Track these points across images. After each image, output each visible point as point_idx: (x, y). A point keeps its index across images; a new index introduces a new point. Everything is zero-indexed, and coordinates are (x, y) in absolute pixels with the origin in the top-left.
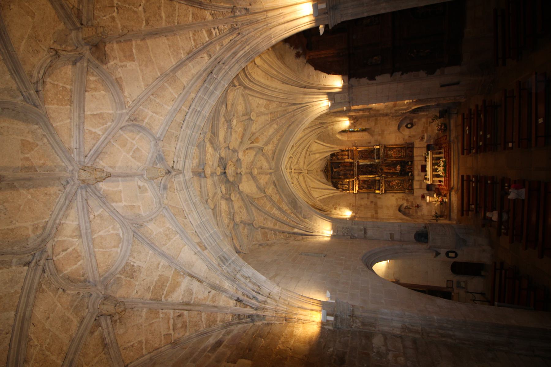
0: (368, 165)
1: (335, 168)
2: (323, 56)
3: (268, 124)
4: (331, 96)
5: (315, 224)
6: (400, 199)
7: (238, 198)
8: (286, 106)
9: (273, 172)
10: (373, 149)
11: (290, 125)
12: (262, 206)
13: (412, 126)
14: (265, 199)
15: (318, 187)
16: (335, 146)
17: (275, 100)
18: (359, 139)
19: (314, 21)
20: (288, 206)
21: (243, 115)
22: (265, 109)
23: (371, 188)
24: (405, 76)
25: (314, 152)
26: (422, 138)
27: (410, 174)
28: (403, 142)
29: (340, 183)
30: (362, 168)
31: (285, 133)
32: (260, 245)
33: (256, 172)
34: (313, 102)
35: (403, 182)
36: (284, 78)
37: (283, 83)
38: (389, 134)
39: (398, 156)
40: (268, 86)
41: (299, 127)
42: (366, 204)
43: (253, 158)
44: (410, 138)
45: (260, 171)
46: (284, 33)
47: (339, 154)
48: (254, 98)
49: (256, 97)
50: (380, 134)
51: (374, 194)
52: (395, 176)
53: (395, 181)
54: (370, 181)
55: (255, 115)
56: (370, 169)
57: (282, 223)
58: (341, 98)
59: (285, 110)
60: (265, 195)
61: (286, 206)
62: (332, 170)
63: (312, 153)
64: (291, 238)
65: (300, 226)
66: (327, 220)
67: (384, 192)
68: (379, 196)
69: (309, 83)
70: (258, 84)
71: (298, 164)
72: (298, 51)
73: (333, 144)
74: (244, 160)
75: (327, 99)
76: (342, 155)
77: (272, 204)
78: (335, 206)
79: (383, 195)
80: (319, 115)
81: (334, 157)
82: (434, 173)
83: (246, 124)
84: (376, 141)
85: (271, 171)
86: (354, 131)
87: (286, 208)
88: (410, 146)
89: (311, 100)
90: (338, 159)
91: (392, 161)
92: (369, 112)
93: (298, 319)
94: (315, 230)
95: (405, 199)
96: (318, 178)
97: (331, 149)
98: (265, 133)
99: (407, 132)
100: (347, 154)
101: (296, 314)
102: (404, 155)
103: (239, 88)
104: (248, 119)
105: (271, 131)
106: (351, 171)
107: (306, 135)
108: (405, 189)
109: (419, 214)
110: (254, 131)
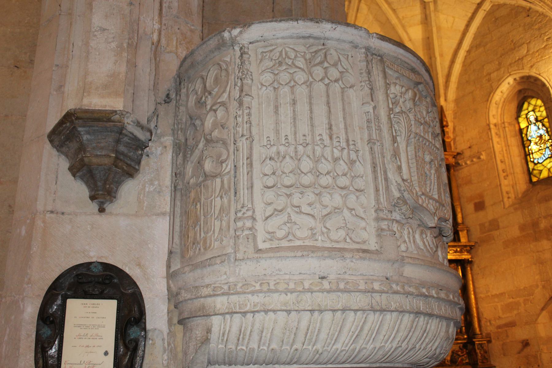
16: (452, 94)
18: (499, 162)
44: (520, 346)
50: (535, 224)
84: (494, 225)
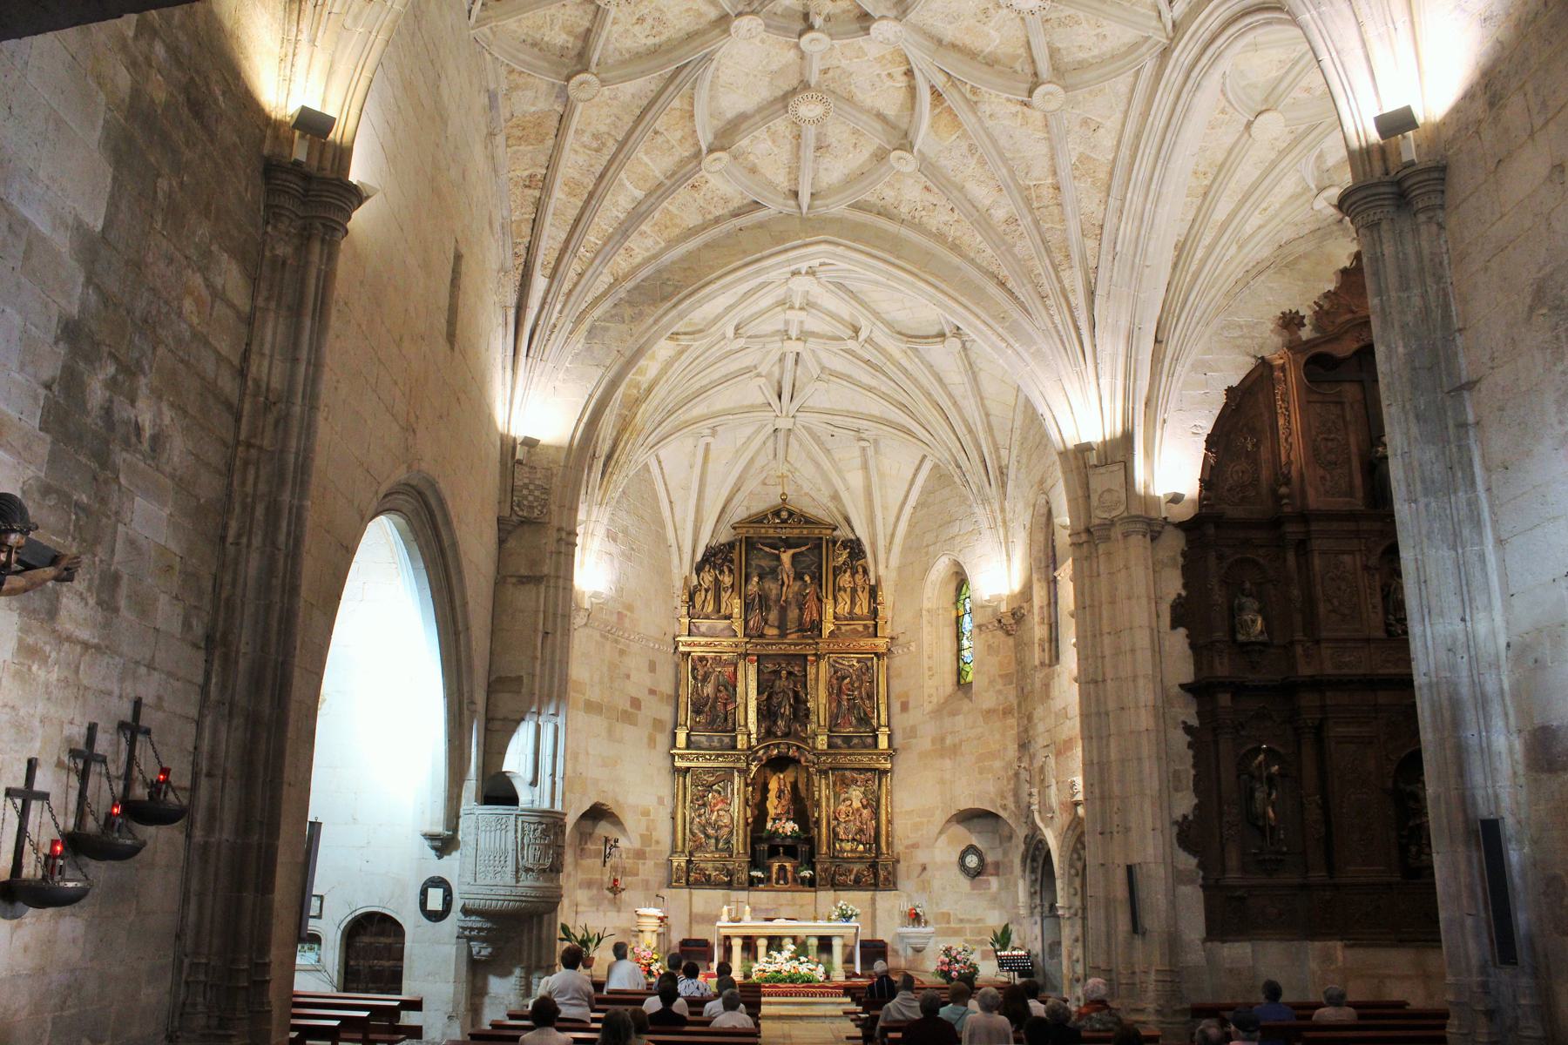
0: (806, 701)
1: (794, 556)
2: (1281, 422)
3: (1012, 172)
4: (1119, 452)
5: (560, 376)
6: (647, 829)
7: (701, 15)
8: (1084, 259)
9: (799, 207)
10: (875, 722)
11: (1002, 284)
12: (656, 133)
13: (975, 874)
14: (687, 154)
15: (710, 478)
16: (895, 560)
19: (1364, 144)
20: (647, 261)
21: (1053, 53)
23: (697, 711)
24: (1180, 740)
25: (872, 463)
26: (915, 918)
27: (759, 874)
28: (899, 847)
29: (727, 580)
30: (790, 673)
31: (972, 261)
32: (492, 97)
33: (808, 109)
34: (1098, 378)
35: (721, 845)
36: (1200, 254)
37: (1180, 248)
38: (942, 782)
39: (841, 830)
40: (1168, 160)
41: (996, 326)
42: (628, 677)
43: (868, 103)
45: (810, 133)
46: (1332, 50)
47: (859, 577)
48: (1122, 107)
49: (1126, 114)
50: (943, 739)
51: (669, 726)
52: (749, 814)
53: (733, 810)
54: (730, 708)
55: (1053, 106)
56: (786, 710)
57: (577, 221)
58: (1109, 490)
59: (1068, 256)
60: (704, 149)
61: (647, 254)
62: (788, 544)
63: (870, 452)
64: (509, 254)
65: (558, 307)
66: (582, 425)
67: (679, 763)
68: (663, 740)
69: (1175, 359)
70: (1179, 108)
71: (823, 376)
72: (1306, 321)
73: (906, 549)
74: (861, 53)
75: (1107, 438)
76: (854, 590)
78: (620, 535)
79: (668, 763)
80: (1042, 409)
81: (844, 555)
82: (762, 944)
83: (1018, 67)
84: (912, 732)
85: (805, 199)
86: (959, 636)
87: (637, 250)
88: (882, 873)
89: (1105, 368)
90: (837, 571)
91: (818, 804)
92: (1042, 664)
93: (297, 41)
94: (538, 372)
95: (648, 849)
96: (752, 484)
97: (881, 543)
98: (973, 162)
99: (944, 852)
100: (857, 610)
101: (313, 42)
102: (842, 850)
103: (1165, 27)
104: (1036, 74)
105: (982, 194)
106: (779, 628)
107: (955, 403)
108: (691, 854)
109: (582, 896)
110: (986, 109)
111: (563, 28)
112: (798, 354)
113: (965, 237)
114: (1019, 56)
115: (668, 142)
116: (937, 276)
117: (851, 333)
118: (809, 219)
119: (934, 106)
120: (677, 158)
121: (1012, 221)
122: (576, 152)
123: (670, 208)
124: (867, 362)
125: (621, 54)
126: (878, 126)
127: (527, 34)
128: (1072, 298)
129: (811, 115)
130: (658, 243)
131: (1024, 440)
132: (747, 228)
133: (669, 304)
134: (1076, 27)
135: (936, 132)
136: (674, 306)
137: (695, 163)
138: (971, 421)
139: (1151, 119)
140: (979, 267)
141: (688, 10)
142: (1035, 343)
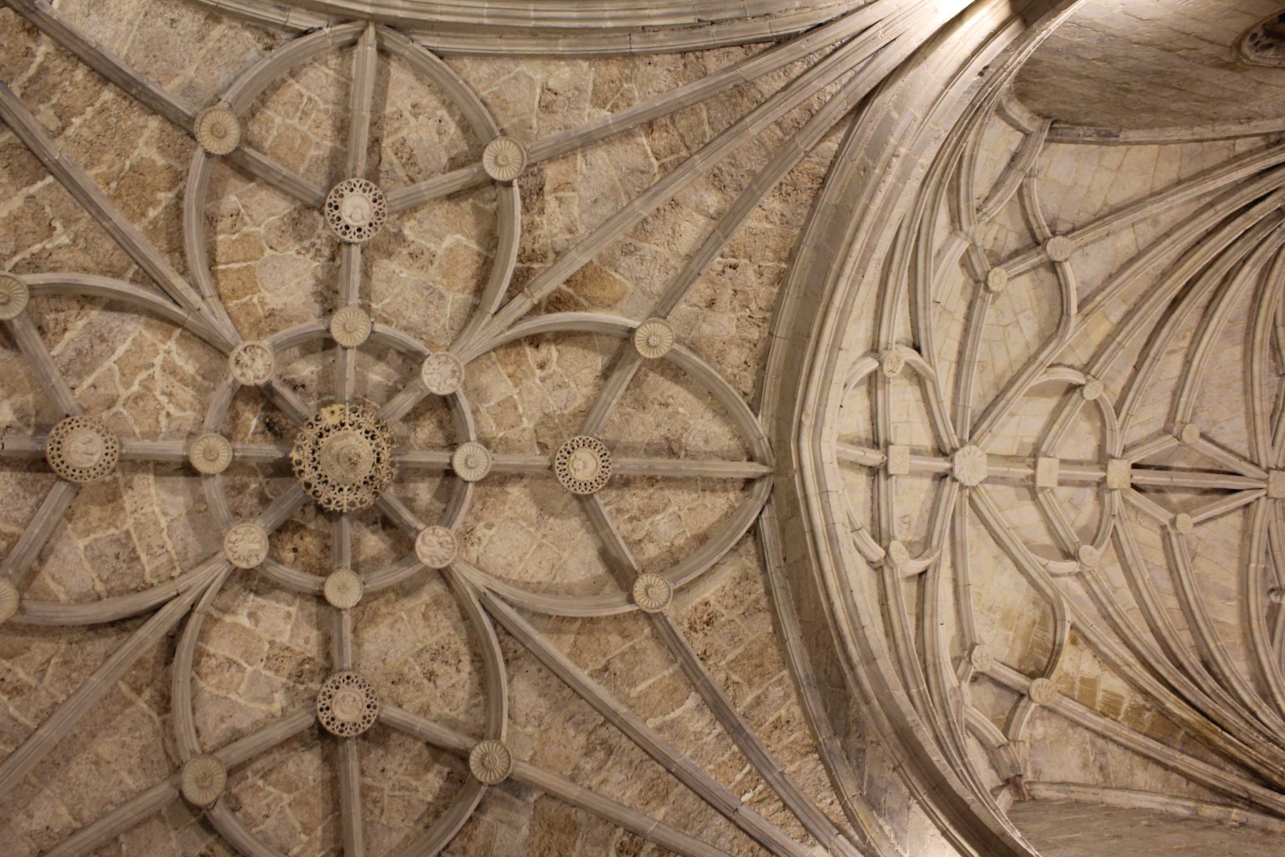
7: (436, 602)
9: (763, 476)
14: (647, 630)
17: (636, 48)
20: (801, 701)
21: (455, 164)
22: (605, 113)
31: (804, 229)
43: (587, 391)
45: (628, 464)
48: (510, 65)
49: (514, 57)
60: (629, 608)
61: (794, 698)
71: (1175, 430)
77: (682, 666)
83: (490, 207)
98: (647, 248)
105: (690, 229)
110: (561, 239)
111: (417, 776)
112: (1135, 466)
113: (771, 243)
114: (475, 207)
115: (623, 654)
116: (826, 277)
117: (1076, 396)
118: (777, 464)
119: (577, 306)
120: (651, 644)
121: (715, 179)
122: (604, 781)
123: (730, 657)
124: (1137, 368)
125: (476, 706)
126: (616, 376)
127: (416, 822)
128: (798, 68)
129: (592, 465)
130: (780, 681)
131: (1199, 119)
132: (784, 550)
133: (849, 677)
134: (409, 143)
135: (616, 301)
136: (852, 668)
137: (655, 621)
138: (1194, 207)
139: (486, 21)
140: (809, 219)
141: (425, 617)
142: (888, 115)
